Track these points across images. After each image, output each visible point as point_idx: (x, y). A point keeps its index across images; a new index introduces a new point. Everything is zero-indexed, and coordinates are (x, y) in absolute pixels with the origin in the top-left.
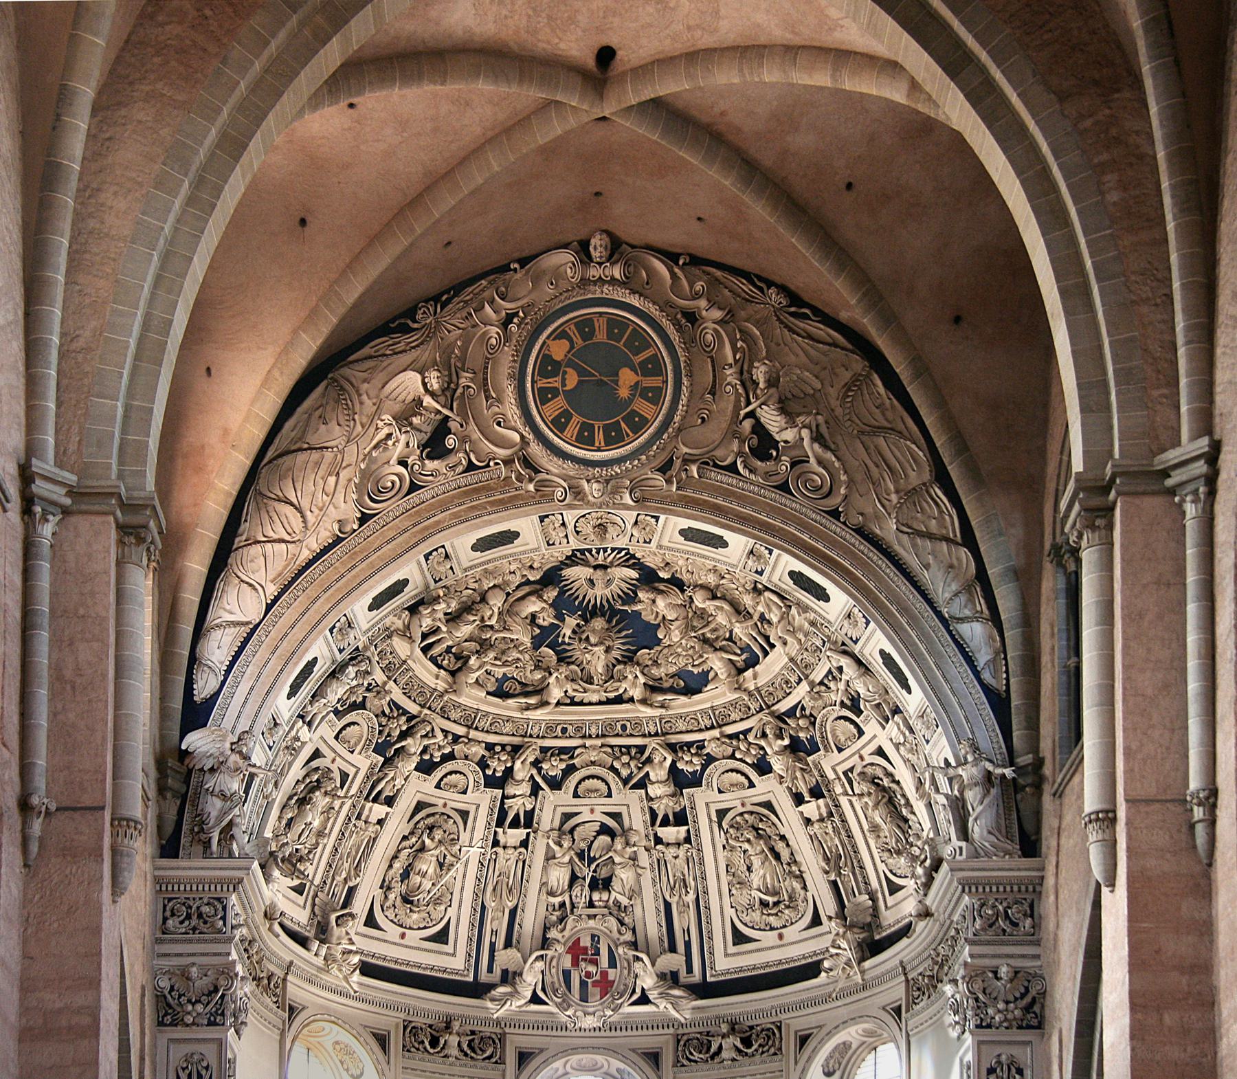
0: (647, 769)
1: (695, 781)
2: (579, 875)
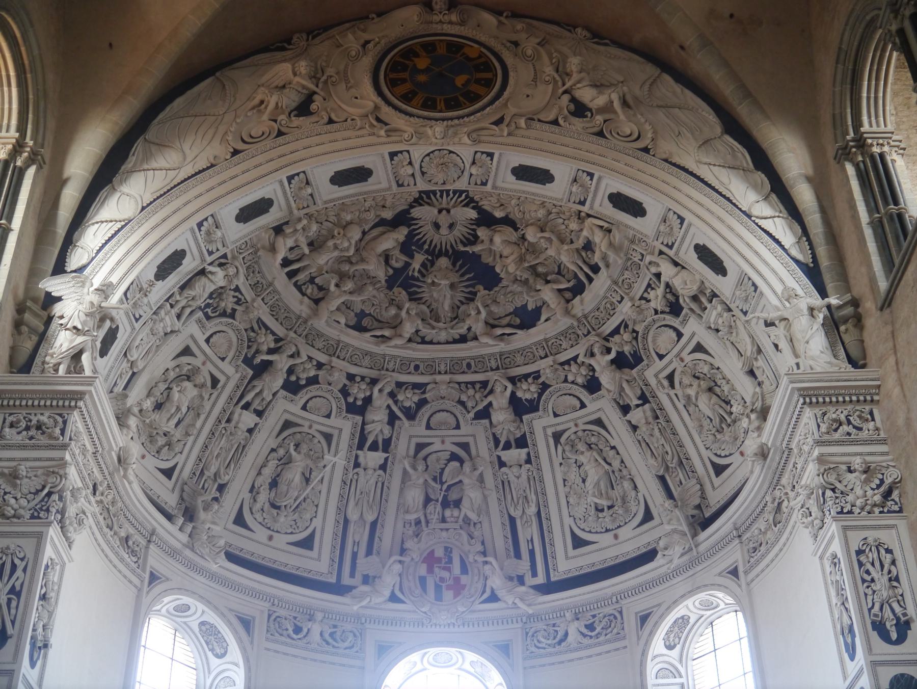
0: (490, 398)
1: (533, 406)
2: (432, 497)
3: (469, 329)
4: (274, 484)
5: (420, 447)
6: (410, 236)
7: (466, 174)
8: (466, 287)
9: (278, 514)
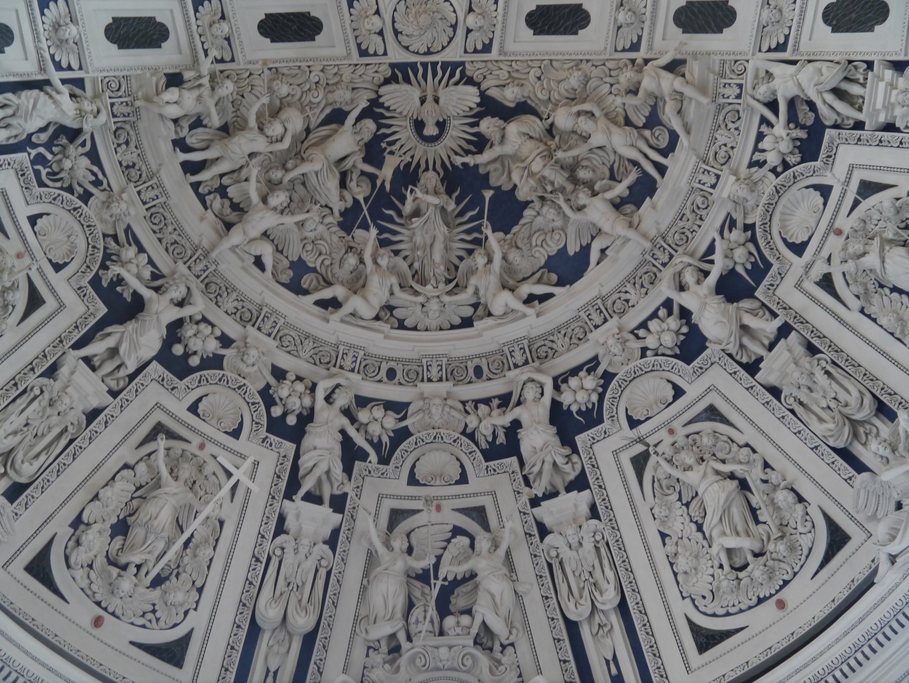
3: (475, 306)
4: (121, 528)
5: (397, 516)
6: (377, 138)
7: (461, 32)
8: (468, 232)
9: (119, 575)
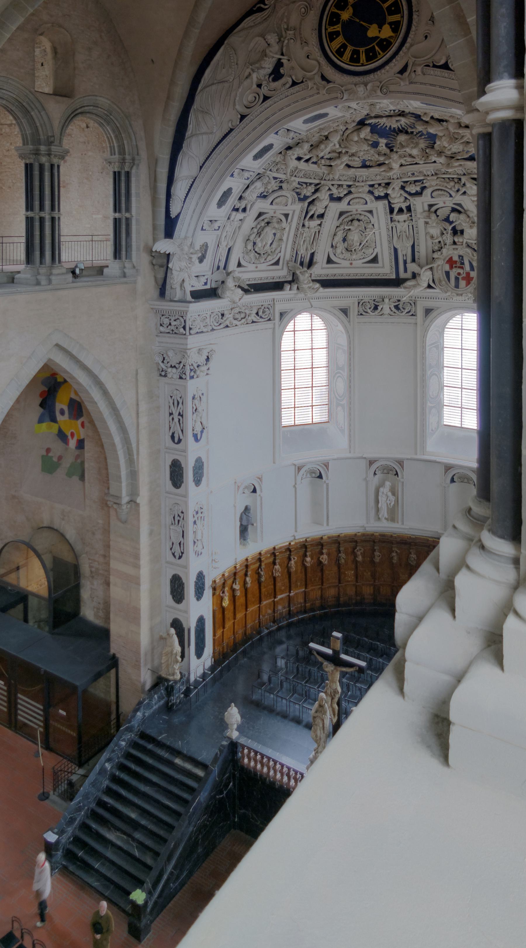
4: (344, 240)
